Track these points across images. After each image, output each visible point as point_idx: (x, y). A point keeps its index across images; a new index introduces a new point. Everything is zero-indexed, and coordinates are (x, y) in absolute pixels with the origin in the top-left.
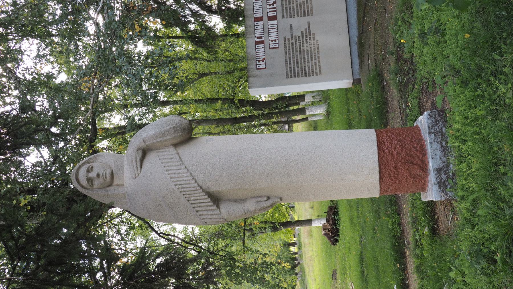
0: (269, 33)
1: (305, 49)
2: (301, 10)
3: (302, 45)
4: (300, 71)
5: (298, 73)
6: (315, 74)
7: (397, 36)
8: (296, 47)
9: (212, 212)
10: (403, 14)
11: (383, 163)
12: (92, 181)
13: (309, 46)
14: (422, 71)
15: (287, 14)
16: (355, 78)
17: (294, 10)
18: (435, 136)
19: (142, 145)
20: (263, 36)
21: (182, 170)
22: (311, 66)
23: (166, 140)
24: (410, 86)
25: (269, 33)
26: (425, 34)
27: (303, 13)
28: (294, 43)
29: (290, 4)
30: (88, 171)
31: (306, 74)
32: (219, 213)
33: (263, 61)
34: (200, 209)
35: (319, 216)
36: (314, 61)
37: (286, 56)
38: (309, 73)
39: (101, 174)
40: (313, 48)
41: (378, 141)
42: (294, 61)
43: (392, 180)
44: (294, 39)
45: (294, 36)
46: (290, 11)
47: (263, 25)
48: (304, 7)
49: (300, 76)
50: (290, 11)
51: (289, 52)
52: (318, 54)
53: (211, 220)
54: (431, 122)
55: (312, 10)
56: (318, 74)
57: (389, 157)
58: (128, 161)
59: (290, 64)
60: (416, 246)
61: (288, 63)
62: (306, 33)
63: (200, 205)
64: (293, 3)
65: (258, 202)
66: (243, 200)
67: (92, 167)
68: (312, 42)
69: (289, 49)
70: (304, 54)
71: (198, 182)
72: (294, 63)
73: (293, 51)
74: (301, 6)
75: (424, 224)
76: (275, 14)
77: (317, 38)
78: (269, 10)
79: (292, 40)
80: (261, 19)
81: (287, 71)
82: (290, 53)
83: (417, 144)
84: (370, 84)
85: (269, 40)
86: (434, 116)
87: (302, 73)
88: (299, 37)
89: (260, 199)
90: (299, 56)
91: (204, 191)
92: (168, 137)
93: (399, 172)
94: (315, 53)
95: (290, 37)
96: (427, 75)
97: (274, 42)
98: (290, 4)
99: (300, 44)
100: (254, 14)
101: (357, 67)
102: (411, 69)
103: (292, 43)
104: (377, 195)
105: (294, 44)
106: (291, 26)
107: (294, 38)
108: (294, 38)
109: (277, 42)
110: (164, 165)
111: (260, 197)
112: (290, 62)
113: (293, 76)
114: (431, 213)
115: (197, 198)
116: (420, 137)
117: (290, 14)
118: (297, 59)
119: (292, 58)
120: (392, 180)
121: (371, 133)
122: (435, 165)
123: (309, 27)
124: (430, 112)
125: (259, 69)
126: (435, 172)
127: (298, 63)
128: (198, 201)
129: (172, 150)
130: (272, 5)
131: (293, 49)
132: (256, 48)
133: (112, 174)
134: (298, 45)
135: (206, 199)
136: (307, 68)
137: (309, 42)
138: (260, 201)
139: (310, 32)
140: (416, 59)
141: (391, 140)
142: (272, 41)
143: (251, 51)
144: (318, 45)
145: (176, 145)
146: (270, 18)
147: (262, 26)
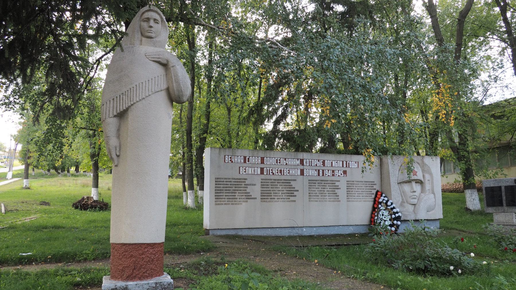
1: (237, 194)
2: (266, 193)
7: (235, 264)
8: (239, 187)
9: (111, 110)
10: (249, 268)
11: (136, 247)
12: (147, 21)
13: (238, 197)
14: (205, 280)
16: (210, 231)
18: (154, 287)
19: (171, 65)
21: (147, 92)
23: (172, 83)
24: (196, 272)
26: (230, 282)
29: (271, 185)
30: (155, 20)
31: (217, 193)
32: (110, 116)
33: (230, 161)
34: (115, 102)
35: (100, 194)
36: (226, 200)
37: (233, 179)
38: (217, 196)
39: (152, 29)
41: (155, 244)
43: (122, 253)
48: (267, 196)
51: (236, 182)
52: (232, 204)
53: (105, 109)
54: (165, 284)
55: (264, 201)
57: (141, 252)
58: (159, 52)
59: (226, 182)
60: (65, 271)
63: (118, 102)
65: (116, 148)
66: (118, 136)
67: (158, 23)
68: (241, 200)
69: (237, 182)
70: (233, 193)
71: (137, 104)
72: (226, 184)
73: (236, 185)
75: (84, 278)
76: (265, 173)
77: (244, 204)
78: (268, 169)
79: (245, 185)
80: (262, 162)
81: (221, 179)
82: (234, 182)
83: (149, 274)
84: (203, 242)
86: (169, 287)
87: (218, 190)
88: (246, 190)
89: (118, 149)
91: (129, 107)
92: (174, 84)
93: (128, 258)
96: (201, 283)
98: (271, 185)
99: (240, 190)
101: (219, 233)
102: (208, 273)
104: (112, 241)
106: (255, 185)
107: (246, 186)
108: (246, 186)
109: (244, 173)
110: (154, 79)
111: (120, 150)
114: (92, 284)
115: (124, 100)
116: (154, 276)
118: (229, 187)
120: (122, 253)
121: (161, 239)
122: (131, 286)
123: (253, 198)
124: (173, 283)
125: (225, 157)
126: (125, 286)
127: (226, 187)
128: (121, 101)
129: (165, 86)
131: (238, 185)
133: (152, 38)
134: (240, 189)
135: (123, 108)
136: (222, 194)
138: (116, 149)
139: (249, 199)
140: (214, 276)
141: (154, 254)
142: (245, 169)
143: (239, 152)
144: (239, 204)
145: (168, 90)
146: (262, 170)
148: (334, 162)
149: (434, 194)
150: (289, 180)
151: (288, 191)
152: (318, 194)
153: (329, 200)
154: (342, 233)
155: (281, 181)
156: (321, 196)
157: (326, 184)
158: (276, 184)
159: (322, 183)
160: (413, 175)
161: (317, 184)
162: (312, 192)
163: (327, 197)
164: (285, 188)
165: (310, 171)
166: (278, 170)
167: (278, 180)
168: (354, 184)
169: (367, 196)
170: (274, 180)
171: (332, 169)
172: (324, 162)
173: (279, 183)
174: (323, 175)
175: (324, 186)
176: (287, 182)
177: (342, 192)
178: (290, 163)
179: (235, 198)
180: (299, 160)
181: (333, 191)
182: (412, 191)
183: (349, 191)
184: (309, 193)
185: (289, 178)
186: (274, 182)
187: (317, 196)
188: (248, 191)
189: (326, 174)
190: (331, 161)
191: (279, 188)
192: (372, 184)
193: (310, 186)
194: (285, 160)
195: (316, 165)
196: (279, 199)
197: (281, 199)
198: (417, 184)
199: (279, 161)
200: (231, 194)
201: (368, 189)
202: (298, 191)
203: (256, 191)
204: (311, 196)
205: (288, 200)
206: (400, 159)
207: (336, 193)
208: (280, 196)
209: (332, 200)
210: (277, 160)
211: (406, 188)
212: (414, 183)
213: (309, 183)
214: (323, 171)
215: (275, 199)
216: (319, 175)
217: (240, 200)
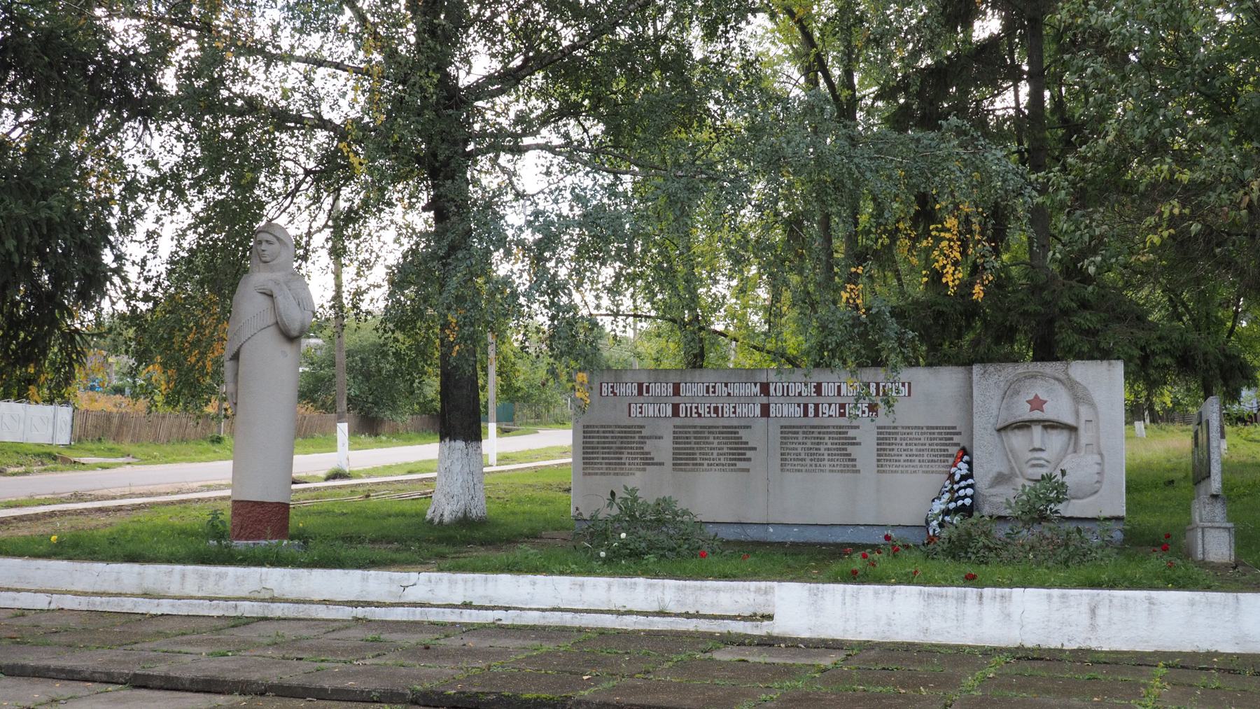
5: (589, 443)
8: (628, 443)
17: (685, 443)
29: (695, 438)
30: (267, 241)
31: (587, 453)
36: (604, 466)
37: (616, 426)
38: (587, 458)
41: (263, 503)
42: (607, 437)
48: (687, 459)
51: (622, 432)
52: (614, 474)
55: (681, 470)
59: (604, 432)
62: (647, 459)
69: (625, 432)
70: (617, 453)
72: (604, 437)
73: (622, 437)
74: (690, 454)
76: (682, 415)
77: (638, 474)
78: (689, 406)
80: (676, 392)
82: (619, 432)
87: (589, 448)
97: (639, 410)
98: (695, 438)
99: (631, 448)
106: (660, 438)
109: (639, 415)
117: (680, 438)
118: (609, 443)
127: (604, 443)
129: (272, 321)
131: (626, 437)
139: (648, 464)
142: (641, 407)
144: (628, 474)
145: (277, 323)
146: (676, 408)
149: (1101, 455)
150: (736, 427)
151: (731, 449)
152: (803, 456)
156: (811, 460)
157: (824, 433)
158: (706, 435)
160: (1032, 410)
161: (801, 435)
163: (826, 462)
166: (709, 407)
167: (710, 427)
168: (897, 433)
169: (932, 461)
170: (701, 427)
172: (818, 388)
174: (816, 415)
176: (731, 432)
177: (865, 453)
178: (736, 391)
179: (622, 464)
181: (840, 449)
183: (884, 450)
184: (782, 454)
185: (735, 423)
186: (701, 433)
187: (802, 460)
188: (646, 450)
189: (823, 413)
192: (948, 433)
193: (785, 438)
194: (726, 385)
195: (800, 394)
198: (1054, 432)
199: (711, 390)
201: (937, 445)
202: (755, 449)
203: (663, 449)
204: (786, 459)
206: (1004, 373)
207: (850, 455)
209: (838, 468)
210: (708, 387)
211: (1017, 440)
212: (1037, 430)
213: (782, 433)
214: (816, 406)
215: (703, 465)
216: (806, 414)
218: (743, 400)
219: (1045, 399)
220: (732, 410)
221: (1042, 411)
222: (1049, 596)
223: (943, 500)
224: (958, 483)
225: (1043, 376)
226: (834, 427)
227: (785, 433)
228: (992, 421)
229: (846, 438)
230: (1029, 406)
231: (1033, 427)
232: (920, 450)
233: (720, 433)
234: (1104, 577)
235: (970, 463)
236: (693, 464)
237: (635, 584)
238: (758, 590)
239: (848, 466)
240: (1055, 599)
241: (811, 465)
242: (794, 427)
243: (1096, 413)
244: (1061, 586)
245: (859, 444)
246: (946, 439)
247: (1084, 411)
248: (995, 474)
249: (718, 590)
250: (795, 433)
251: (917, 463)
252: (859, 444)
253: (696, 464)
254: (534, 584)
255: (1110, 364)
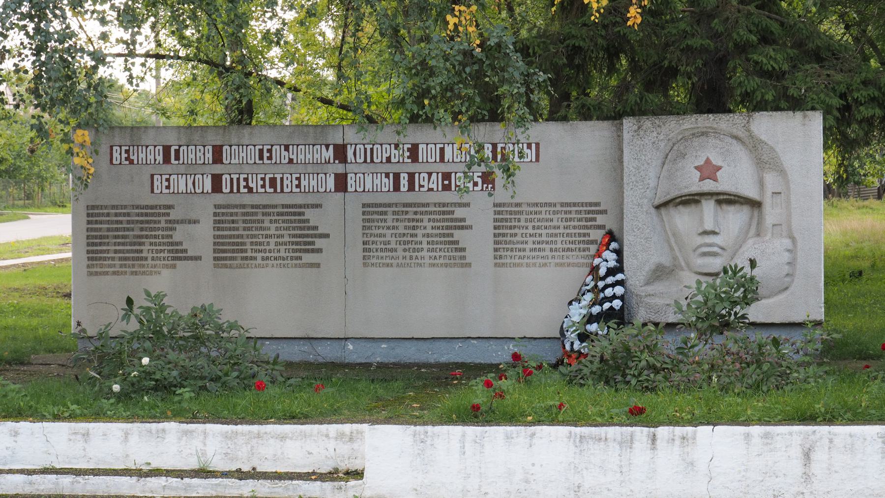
0: (184, 176)
2: (229, 244)
3: (153, 240)
4: (100, 234)
5: (96, 230)
6: (91, 262)
8: (151, 229)
13: (150, 255)
15: (223, 214)
17: (230, 229)
20: (181, 162)
22: (109, 255)
25: (184, 176)
27: (221, 247)
28: (159, 226)
29: (244, 222)
31: (93, 244)
33: (126, 159)
36: (117, 262)
37: (133, 207)
38: (93, 252)
40: (144, 262)
42: (121, 222)
44: (166, 225)
45: (174, 225)
46: (229, 222)
47: (204, 163)
48: (233, 251)
49: (89, 233)
50: (229, 222)
51: (142, 215)
52: (132, 273)
55: (226, 266)
56: (91, 270)
59: (116, 215)
61: (117, 211)
64: (245, 229)
68: (158, 262)
69: (147, 215)
70: (134, 244)
72: (117, 222)
73: (142, 222)
74: (237, 244)
77: (166, 272)
78: (235, 177)
79: (167, 222)
80: (218, 157)
81: (101, 207)
82: (138, 215)
85: (170, 175)
87: (96, 237)
88: (171, 236)
90: (131, 233)
94: (133, 266)
95: (171, 218)
97: (165, 184)
98: (244, 222)
99: (155, 237)
100: (231, 146)
103: (159, 222)
105: (156, 226)
106: (196, 222)
107: (170, 225)
108: (170, 225)
109: (165, 191)
112: (120, 215)
113: (90, 219)
117: (222, 222)
118: (125, 229)
119: (129, 218)
123: (191, 258)
127: (117, 230)
130: (245, 184)
131: (148, 222)
132: (155, 146)
134: (153, 233)
136: (105, 248)
137: (159, 255)
139: (180, 259)
142: (168, 180)
144: (151, 273)
146: (217, 180)
147: (202, 162)
148: (448, 150)
150: (300, 206)
151: (294, 236)
152: (393, 246)
153: (432, 261)
154: (478, 361)
155: (275, 210)
156: (405, 250)
157: (422, 213)
158: (260, 217)
159: (407, 213)
160: (702, 179)
161: (390, 217)
162: (372, 239)
163: (424, 253)
164: (287, 229)
165: (368, 179)
166: (263, 179)
167: (265, 207)
168: (521, 213)
169: (568, 250)
170: (253, 207)
171: (444, 168)
172: (414, 152)
173: (269, 214)
175: (413, 220)
176: (294, 213)
179: (141, 259)
180: (331, 148)
181: (444, 235)
182: (701, 231)
183: (504, 235)
184: (364, 243)
185: (299, 200)
186: (253, 214)
187: (391, 250)
188: (177, 237)
189: (421, 186)
190: (438, 146)
191: (269, 229)
192: (589, 212)
193: (368, 221)
194: (287, 148)
195: (389, 160)
196: (267, 258)
197: (275, 259)
198: (731, 209)
199: (266, 155)
200: (129, 248)
201: (574, 227)
202: (327, 236)
204: (370, 250)
205: (294, 262)
206: (664, 129)
207: (457, 242)
208: (270, 251)
209: (442, 261)
210: (261, 151)
212: (708, 207)
213: (364, 213)
214: (411, 176)
215: (255, 258)
216: (397, 188)
217: (153, 262)
218: (310, 169)
219: (719, 164)
220: (295, 182)
221: (716, 180)
222: (748, 436)
223: (583, 303)
224: (603, 279)
225: (717, 133)
226: (435, 204)
227: (369, 213)
228: (649, 194)
229: (452, 220)
230: (698, 174)
231: (703, 202)
232: (552, 235)
233: (279, 214)
234: (819, 407)
235: (619, 252)
236: (243, 258)
237: (164, 430)
238: (340, 436)
239: (454, 258)
240: (756, 440)
241: (404, 258)
242: (380, 205)
243: (787, 182)
244: (761, 422)
245: (471, 227)
246: (587, 220)
247: (771, 180)
248: (653, 267)
249: (283, 438)
250: (382, 213)
251: (548, 253)
252: (471, 227)
253: (246, 258)
254: (16, 434)
255: (805, 117)
